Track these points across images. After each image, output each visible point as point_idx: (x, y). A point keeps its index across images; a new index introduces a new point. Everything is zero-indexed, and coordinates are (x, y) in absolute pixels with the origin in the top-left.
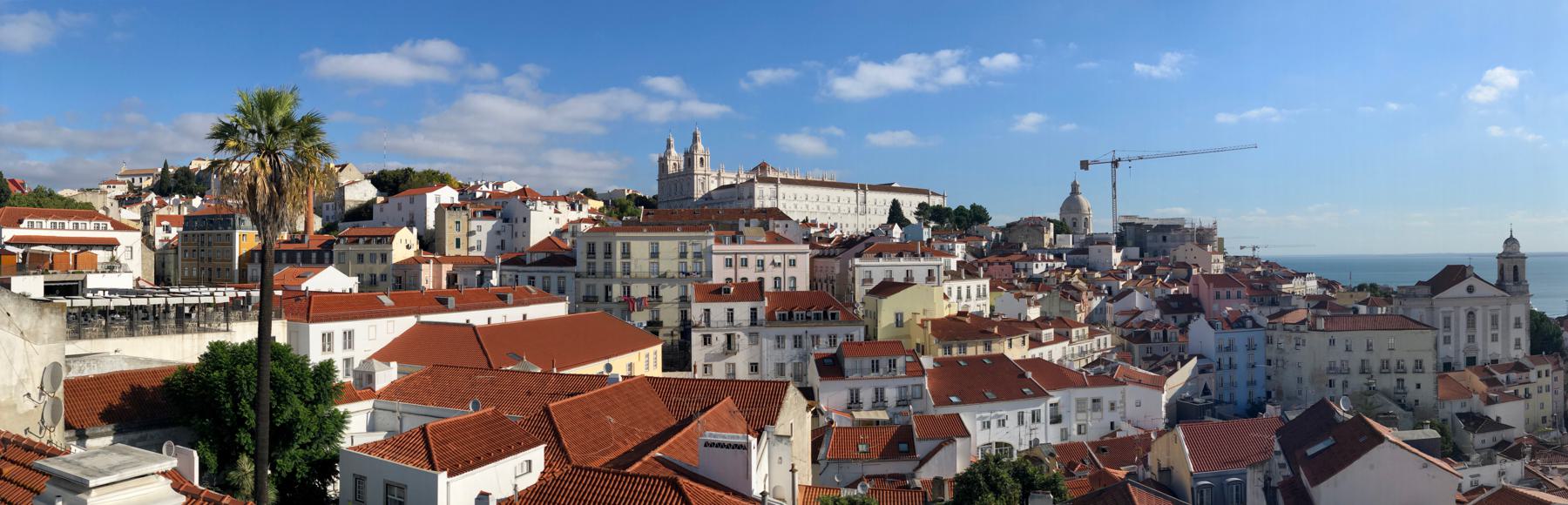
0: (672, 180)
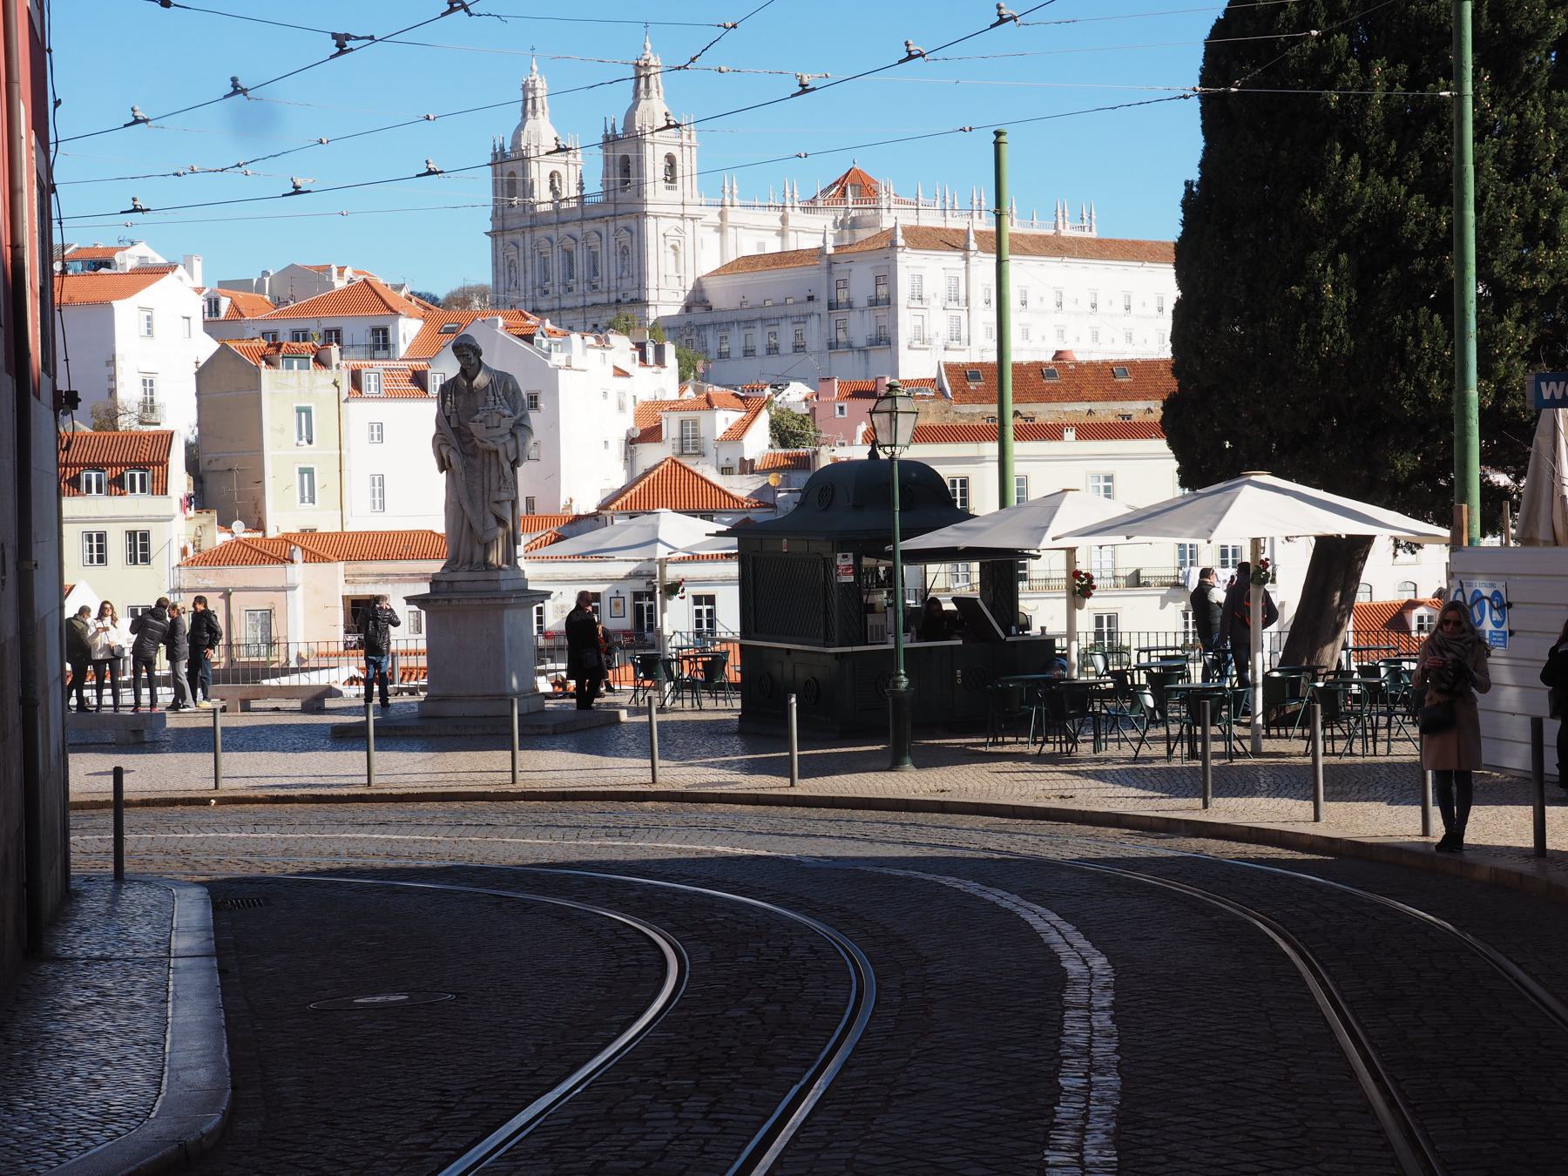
0: (551, 232)
